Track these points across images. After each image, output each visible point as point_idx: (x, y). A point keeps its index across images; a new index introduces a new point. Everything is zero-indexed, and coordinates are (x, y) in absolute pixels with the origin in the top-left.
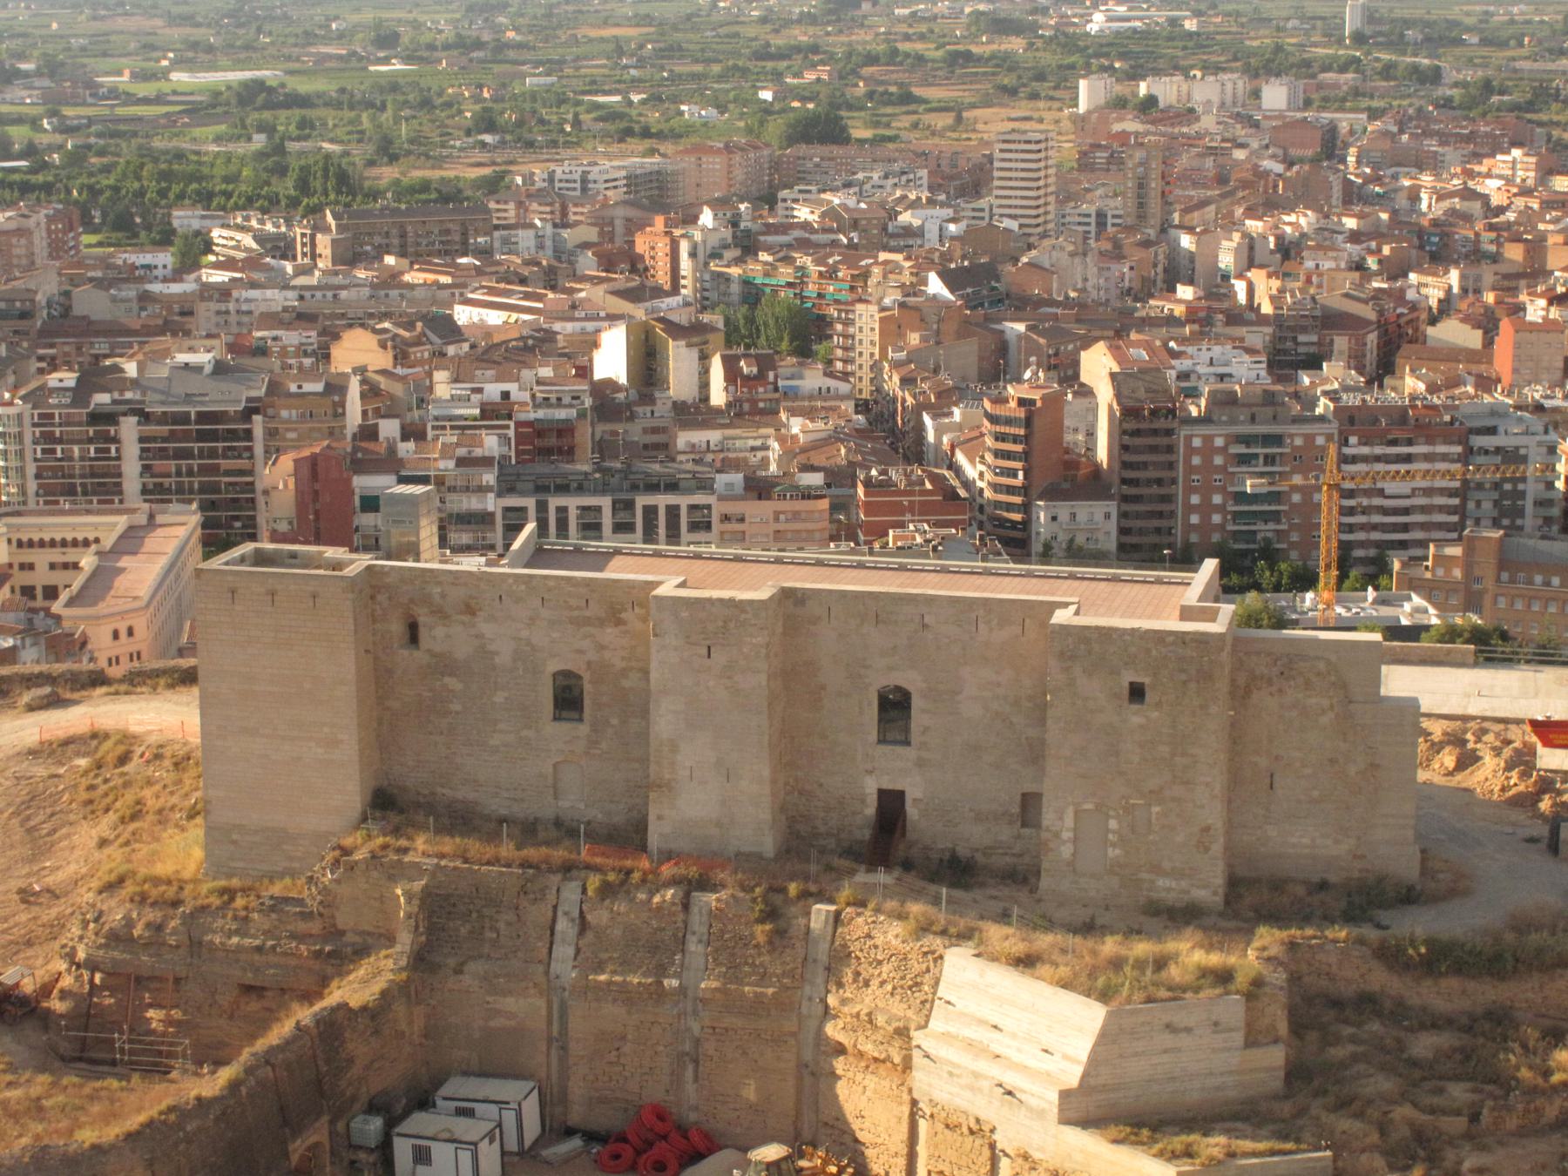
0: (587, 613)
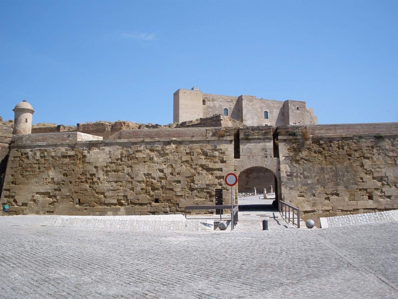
0: (229, 101)
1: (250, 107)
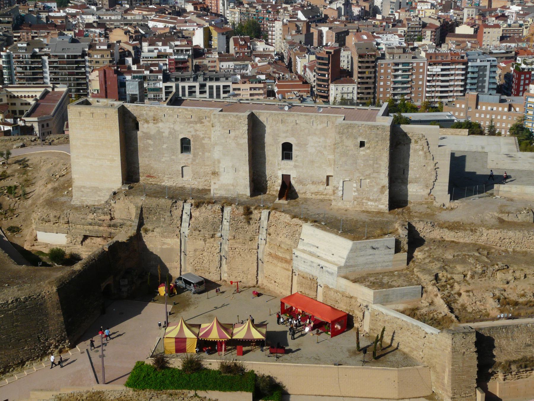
0: (192, 120)
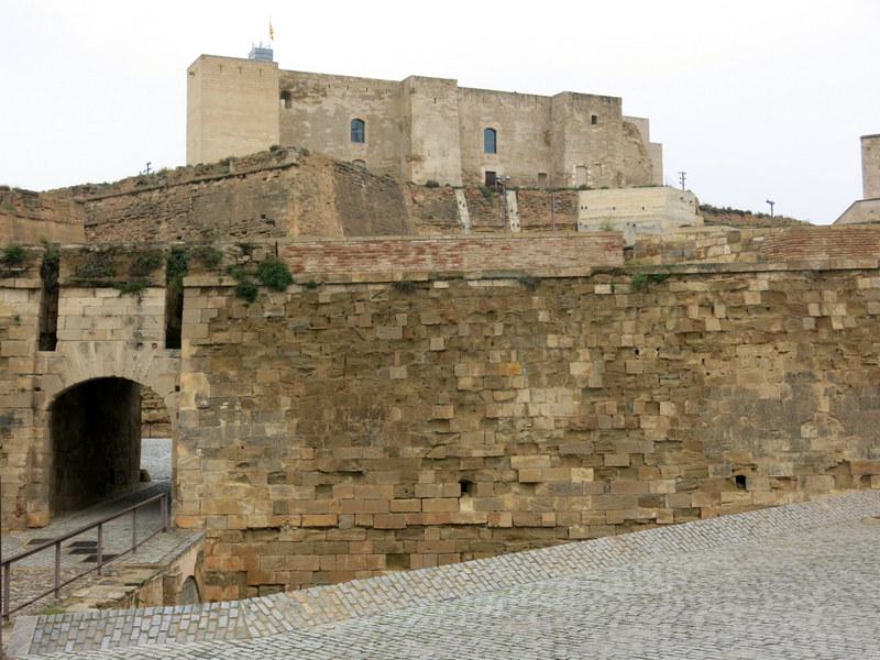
1: (437, 118)
